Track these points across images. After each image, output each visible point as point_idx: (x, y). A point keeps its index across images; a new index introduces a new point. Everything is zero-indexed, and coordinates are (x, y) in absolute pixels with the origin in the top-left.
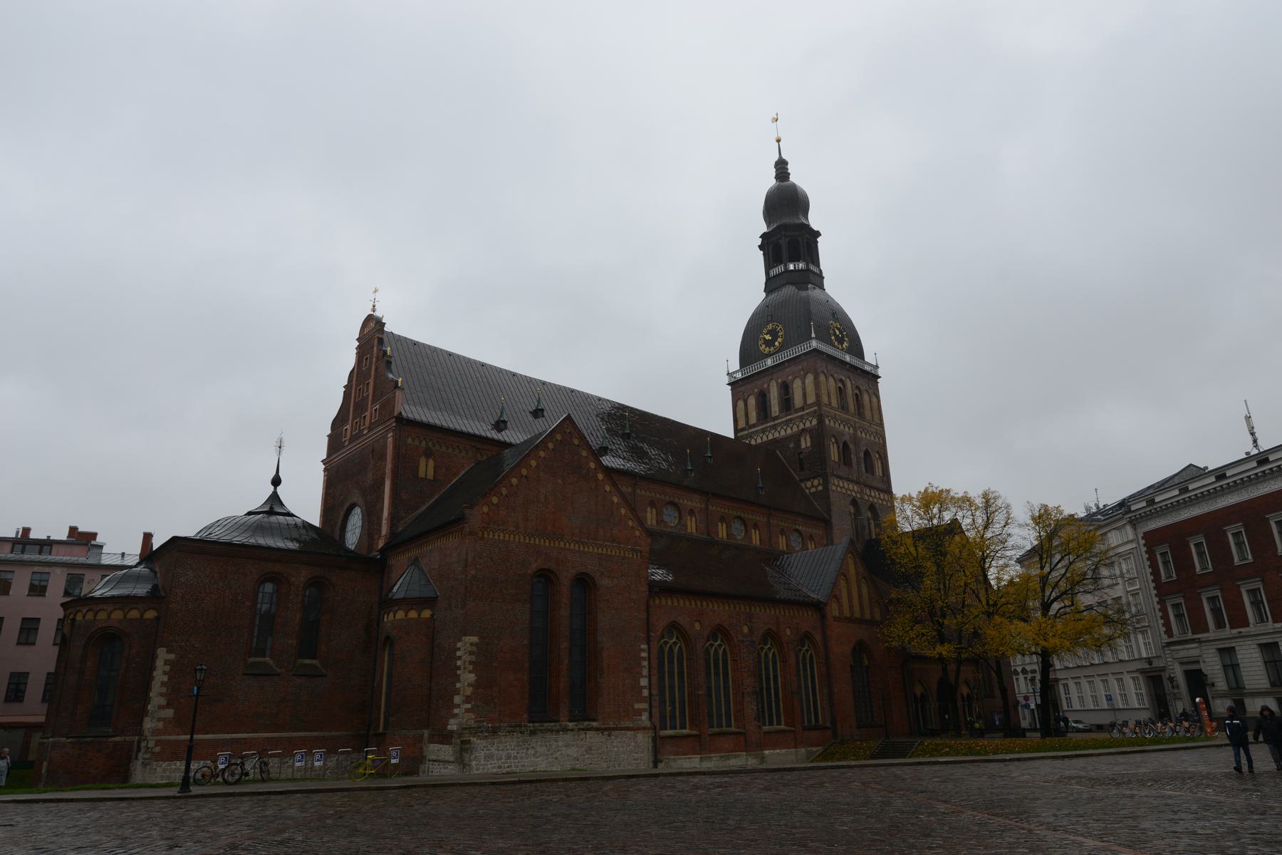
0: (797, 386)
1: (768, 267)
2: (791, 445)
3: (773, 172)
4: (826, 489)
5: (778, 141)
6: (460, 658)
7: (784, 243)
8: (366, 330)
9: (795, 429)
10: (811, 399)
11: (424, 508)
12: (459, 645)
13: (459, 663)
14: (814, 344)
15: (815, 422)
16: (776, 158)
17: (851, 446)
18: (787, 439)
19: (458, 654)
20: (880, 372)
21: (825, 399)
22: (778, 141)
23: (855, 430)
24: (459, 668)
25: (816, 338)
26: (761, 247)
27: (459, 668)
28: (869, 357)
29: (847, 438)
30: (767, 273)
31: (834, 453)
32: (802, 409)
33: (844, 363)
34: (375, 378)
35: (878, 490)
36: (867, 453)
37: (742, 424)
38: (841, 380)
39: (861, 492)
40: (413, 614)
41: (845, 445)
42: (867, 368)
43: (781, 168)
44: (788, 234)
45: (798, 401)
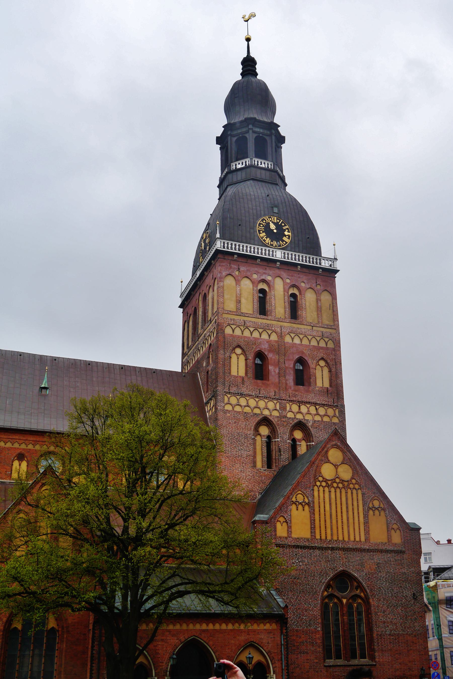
0: (210, 297)
2: (204, 365)
4: (216, 409)
5: (248, 40)
9: (207, 345)
10: (215, 310)
14: (219, 245)
15: (215, 335)
17: (270, 356)
18: (202, 358)
20: (338, 265)
21: (231, 305)
22: (248, 40)
23: (281, 336)
25: (220, 238)
28: (326, 250)
29: (264, 347)
31: (238, 366)
33: (270, 262)
35: (315, 404)
36: (301, 361)
37: (186, 350)
38: (264, 281)
39: (283, 408)
41: (260, 355)
42: (325, 264)
43: (249, 65)
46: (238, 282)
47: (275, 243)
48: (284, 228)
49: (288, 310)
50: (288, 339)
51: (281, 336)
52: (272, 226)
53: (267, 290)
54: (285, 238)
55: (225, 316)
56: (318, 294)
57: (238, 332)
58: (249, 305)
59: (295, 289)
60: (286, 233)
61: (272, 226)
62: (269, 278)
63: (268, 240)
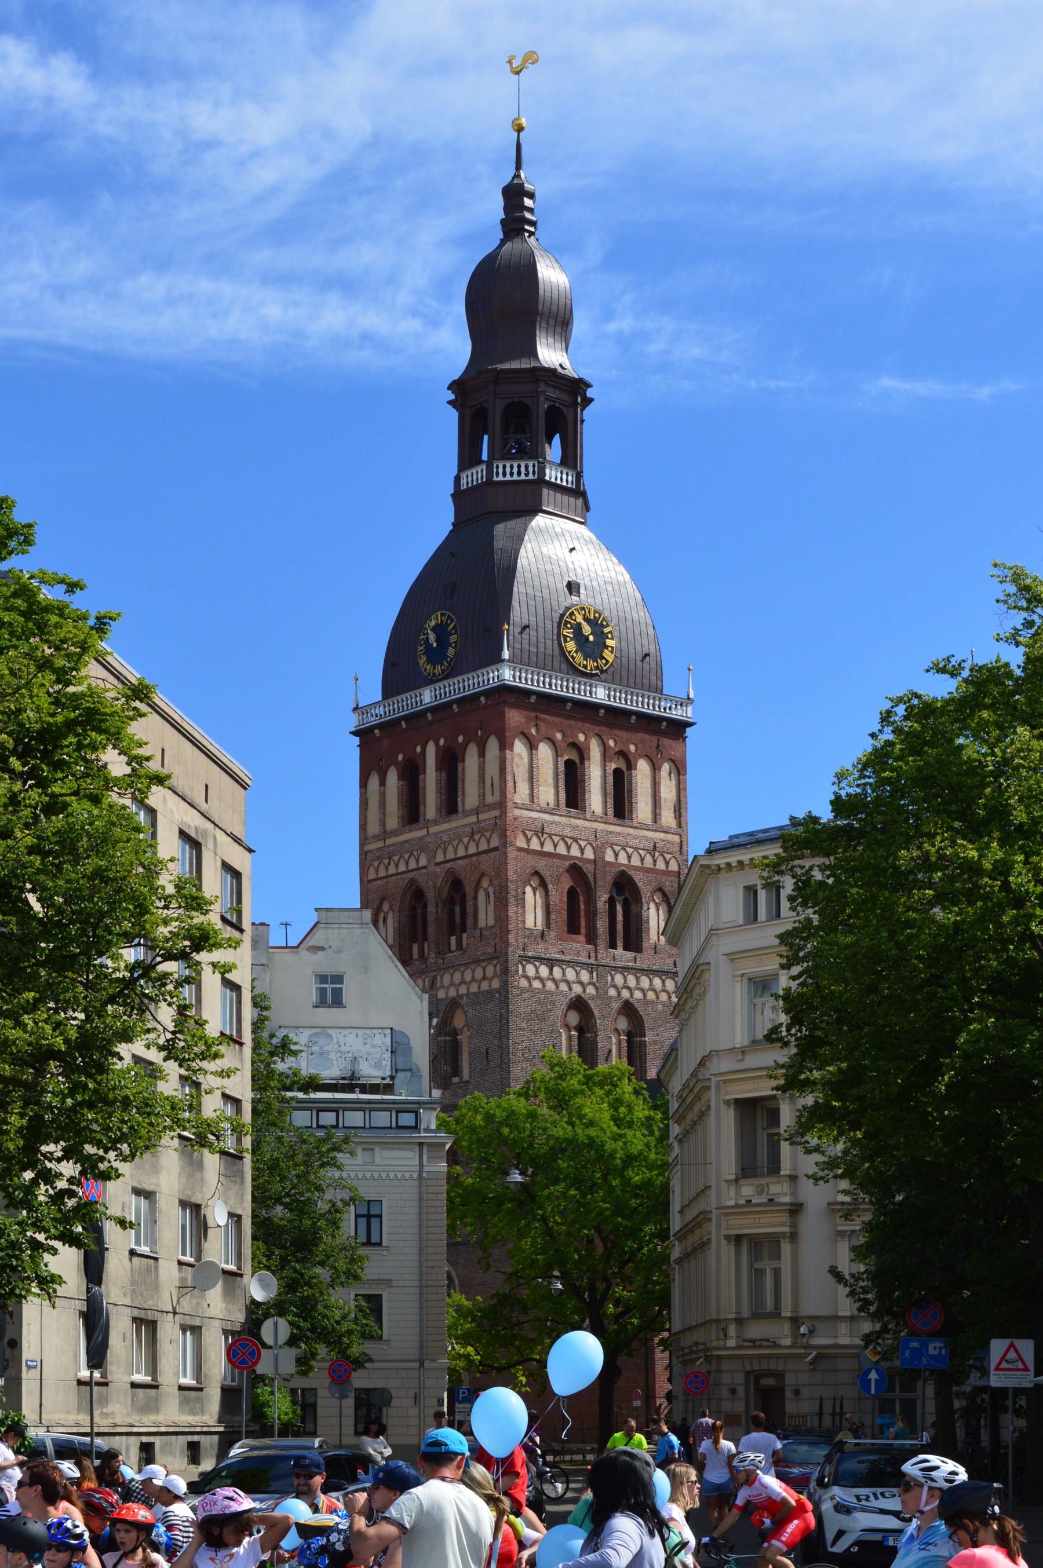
1: (468, 457)
30: (457, 480)
32: (477, 812)
45: (470, 796)
46: (532, 746)
47: (591, 664)
48: (606, 630)
49: (610, 801)
50: (609, 857)
51: (599, 851)
52: (587, 629)
53: (577, 761)
54: (607, 654)
55: (517, 812)
56: (655, 768)
57: (535, 845)
58: (548, 793)
59: (621, 760)
60: (609, 642)
61: (587, 629)
62: (581, 737)
63: (579, 658)
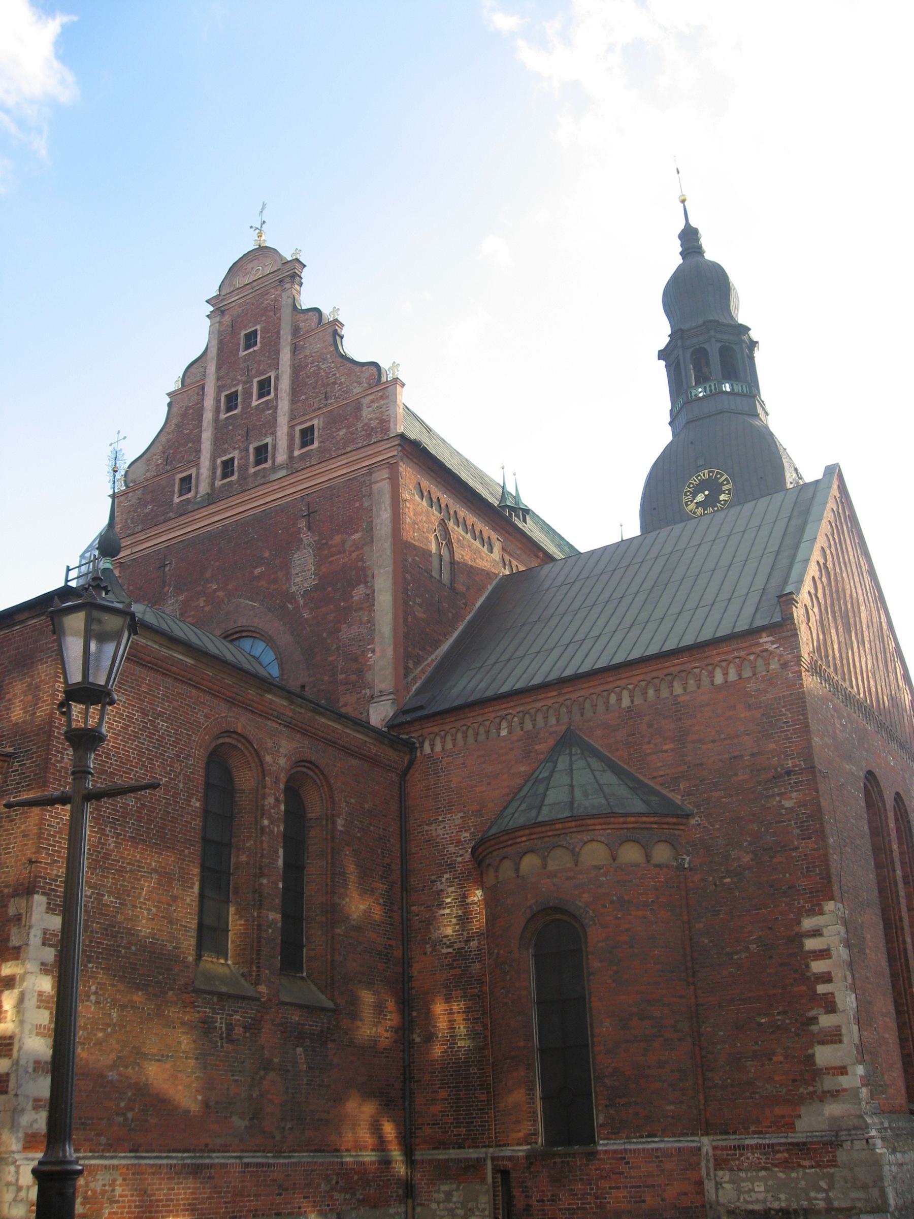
3: (677, 246)
5: (683, 201)
6: (824, 954)
7: (714, 350)
8: (240, 281)
11: (445, 647)
12: (808, 923)
13: (818, 967)
16: (681, 225)
19: (811, 944)
22: (683, 201)
24: (827, 978)
26: (662, 355)
27: (827, 978)
34: (297, 369)
40: (631, 854)
43: (690, 239)
44: (706, 340)
